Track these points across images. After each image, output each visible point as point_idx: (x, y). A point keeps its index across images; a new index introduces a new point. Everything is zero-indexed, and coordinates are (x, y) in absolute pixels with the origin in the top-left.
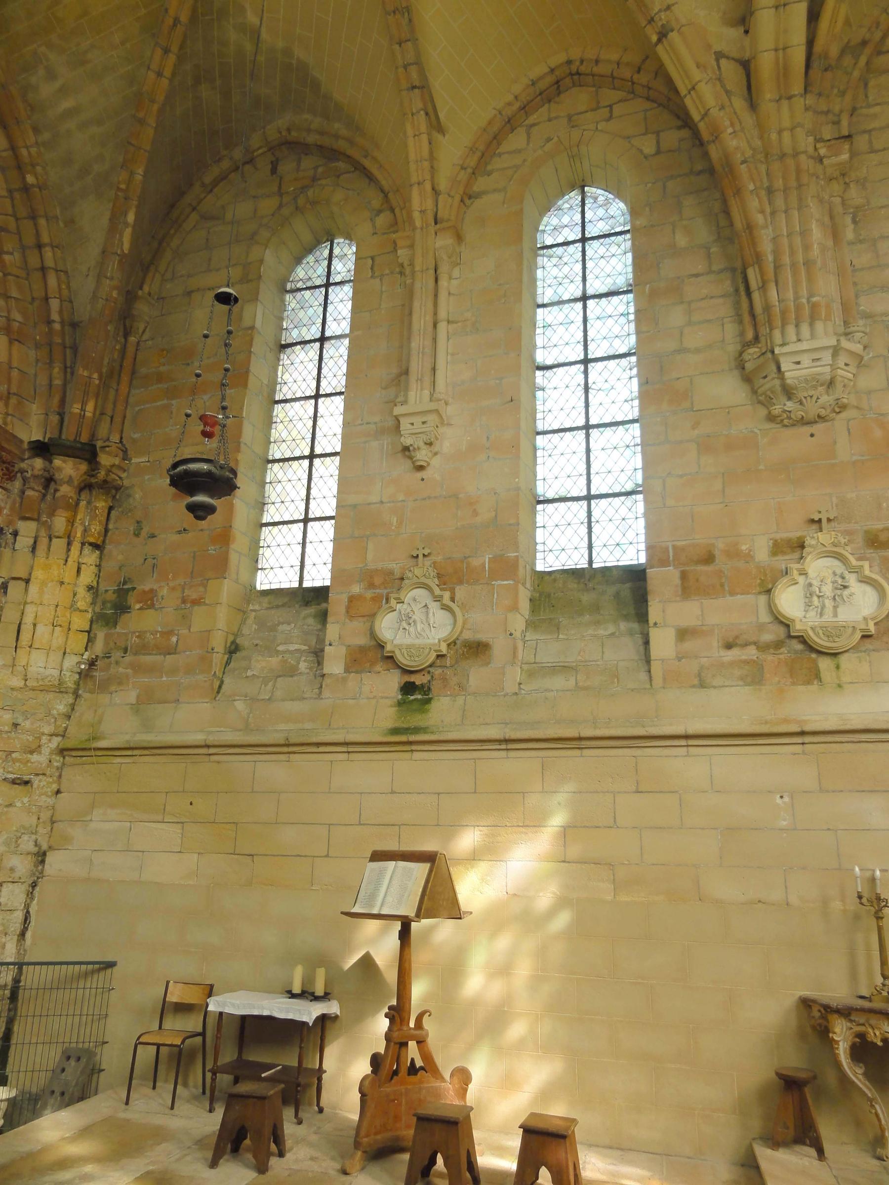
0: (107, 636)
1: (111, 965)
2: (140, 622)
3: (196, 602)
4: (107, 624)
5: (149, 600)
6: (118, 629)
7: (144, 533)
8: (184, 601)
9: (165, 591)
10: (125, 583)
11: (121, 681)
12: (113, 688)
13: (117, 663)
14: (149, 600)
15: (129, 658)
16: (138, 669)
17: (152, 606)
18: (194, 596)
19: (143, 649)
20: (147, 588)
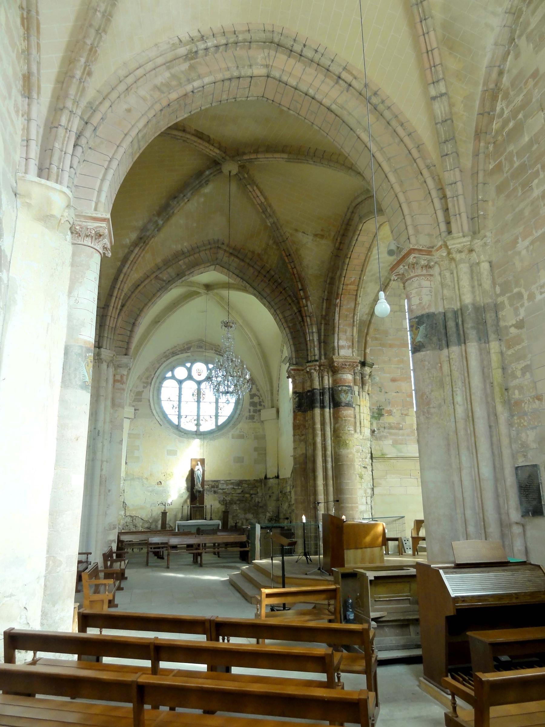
0: (377, 423)
1: (403, 517)
2: (387, 419)
3: (406, 415)
4: (376, 419)
5: (390, 413)
6: (381, 421)
7: (383, 390)
8: (402, 414)
9: (395, 410)
10: (380, 407)
11: (386, 437)
12: (383, 439)
13: (383, 432)
14: (390, 413)
15: (386, 430)
16: (391, 434)
17: (391, 415)
18: (405, 413)
19: (391, 428)
20: (388, 409)
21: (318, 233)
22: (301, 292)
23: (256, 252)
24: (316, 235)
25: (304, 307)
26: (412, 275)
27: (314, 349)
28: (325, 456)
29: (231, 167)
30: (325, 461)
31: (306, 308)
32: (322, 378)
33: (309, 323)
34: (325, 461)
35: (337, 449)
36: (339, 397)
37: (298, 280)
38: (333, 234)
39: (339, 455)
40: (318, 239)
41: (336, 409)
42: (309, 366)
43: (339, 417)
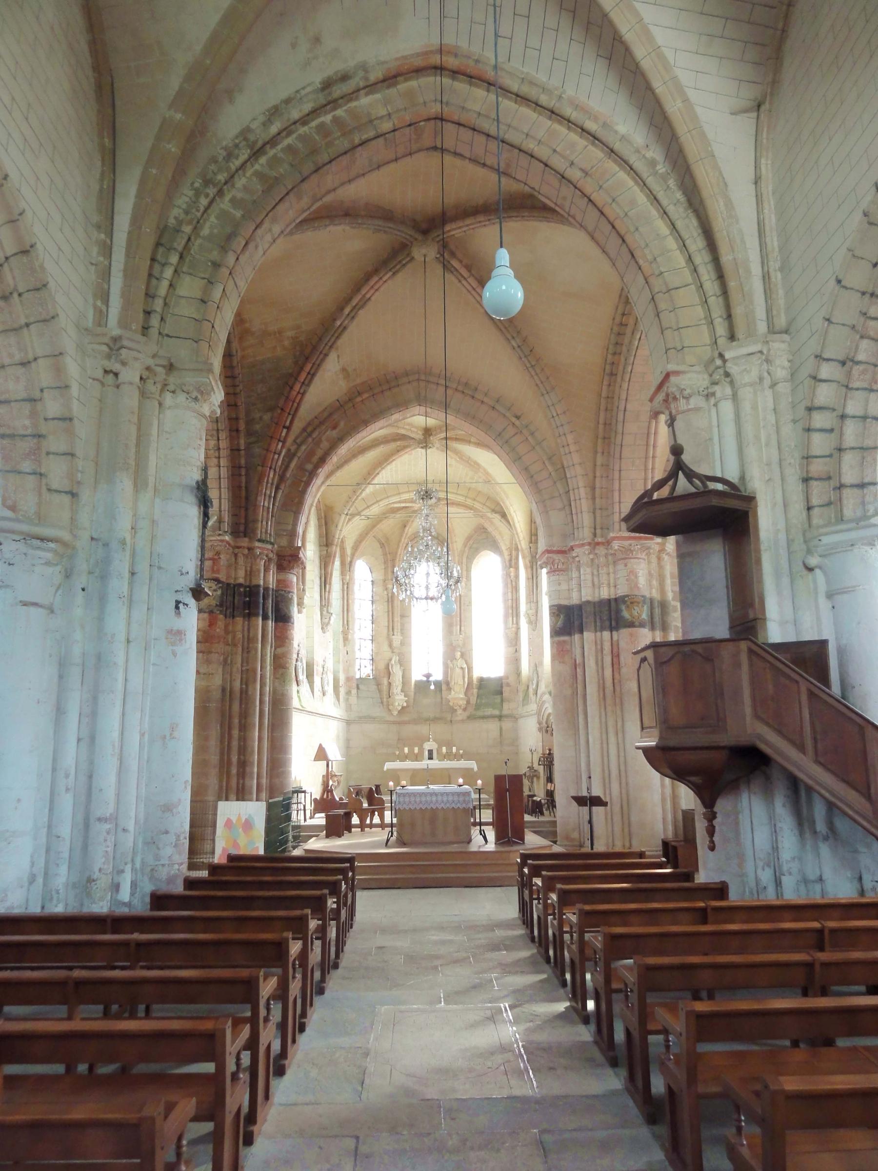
21: (350, 369)
22: (285, 431)
23: (247, 325)
24: (344, 370)
25: (275, 453)
26: (639, 556)
27: (267, 523)
28: (262, 694)
29: (425, 252)
30: (262, 702)
31: (276, 456)
32: (266, 570)
33: (270, 481)
34: (262, 702)
35: (277, 684)
36: (288, 608)
37: (292, 413)
38: (359, 381)
39: (283, 695)
40: (341, 376)
41: (280, 624)
42: (259, 548)
43: (287, 638)
